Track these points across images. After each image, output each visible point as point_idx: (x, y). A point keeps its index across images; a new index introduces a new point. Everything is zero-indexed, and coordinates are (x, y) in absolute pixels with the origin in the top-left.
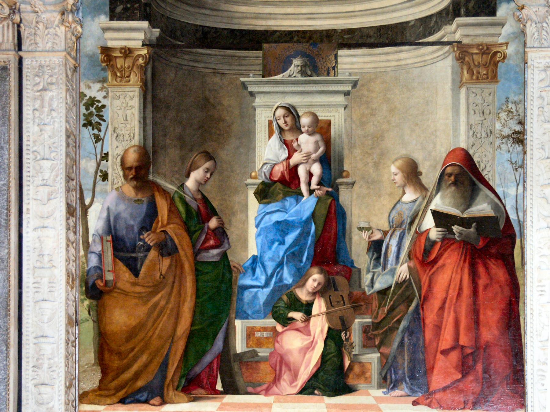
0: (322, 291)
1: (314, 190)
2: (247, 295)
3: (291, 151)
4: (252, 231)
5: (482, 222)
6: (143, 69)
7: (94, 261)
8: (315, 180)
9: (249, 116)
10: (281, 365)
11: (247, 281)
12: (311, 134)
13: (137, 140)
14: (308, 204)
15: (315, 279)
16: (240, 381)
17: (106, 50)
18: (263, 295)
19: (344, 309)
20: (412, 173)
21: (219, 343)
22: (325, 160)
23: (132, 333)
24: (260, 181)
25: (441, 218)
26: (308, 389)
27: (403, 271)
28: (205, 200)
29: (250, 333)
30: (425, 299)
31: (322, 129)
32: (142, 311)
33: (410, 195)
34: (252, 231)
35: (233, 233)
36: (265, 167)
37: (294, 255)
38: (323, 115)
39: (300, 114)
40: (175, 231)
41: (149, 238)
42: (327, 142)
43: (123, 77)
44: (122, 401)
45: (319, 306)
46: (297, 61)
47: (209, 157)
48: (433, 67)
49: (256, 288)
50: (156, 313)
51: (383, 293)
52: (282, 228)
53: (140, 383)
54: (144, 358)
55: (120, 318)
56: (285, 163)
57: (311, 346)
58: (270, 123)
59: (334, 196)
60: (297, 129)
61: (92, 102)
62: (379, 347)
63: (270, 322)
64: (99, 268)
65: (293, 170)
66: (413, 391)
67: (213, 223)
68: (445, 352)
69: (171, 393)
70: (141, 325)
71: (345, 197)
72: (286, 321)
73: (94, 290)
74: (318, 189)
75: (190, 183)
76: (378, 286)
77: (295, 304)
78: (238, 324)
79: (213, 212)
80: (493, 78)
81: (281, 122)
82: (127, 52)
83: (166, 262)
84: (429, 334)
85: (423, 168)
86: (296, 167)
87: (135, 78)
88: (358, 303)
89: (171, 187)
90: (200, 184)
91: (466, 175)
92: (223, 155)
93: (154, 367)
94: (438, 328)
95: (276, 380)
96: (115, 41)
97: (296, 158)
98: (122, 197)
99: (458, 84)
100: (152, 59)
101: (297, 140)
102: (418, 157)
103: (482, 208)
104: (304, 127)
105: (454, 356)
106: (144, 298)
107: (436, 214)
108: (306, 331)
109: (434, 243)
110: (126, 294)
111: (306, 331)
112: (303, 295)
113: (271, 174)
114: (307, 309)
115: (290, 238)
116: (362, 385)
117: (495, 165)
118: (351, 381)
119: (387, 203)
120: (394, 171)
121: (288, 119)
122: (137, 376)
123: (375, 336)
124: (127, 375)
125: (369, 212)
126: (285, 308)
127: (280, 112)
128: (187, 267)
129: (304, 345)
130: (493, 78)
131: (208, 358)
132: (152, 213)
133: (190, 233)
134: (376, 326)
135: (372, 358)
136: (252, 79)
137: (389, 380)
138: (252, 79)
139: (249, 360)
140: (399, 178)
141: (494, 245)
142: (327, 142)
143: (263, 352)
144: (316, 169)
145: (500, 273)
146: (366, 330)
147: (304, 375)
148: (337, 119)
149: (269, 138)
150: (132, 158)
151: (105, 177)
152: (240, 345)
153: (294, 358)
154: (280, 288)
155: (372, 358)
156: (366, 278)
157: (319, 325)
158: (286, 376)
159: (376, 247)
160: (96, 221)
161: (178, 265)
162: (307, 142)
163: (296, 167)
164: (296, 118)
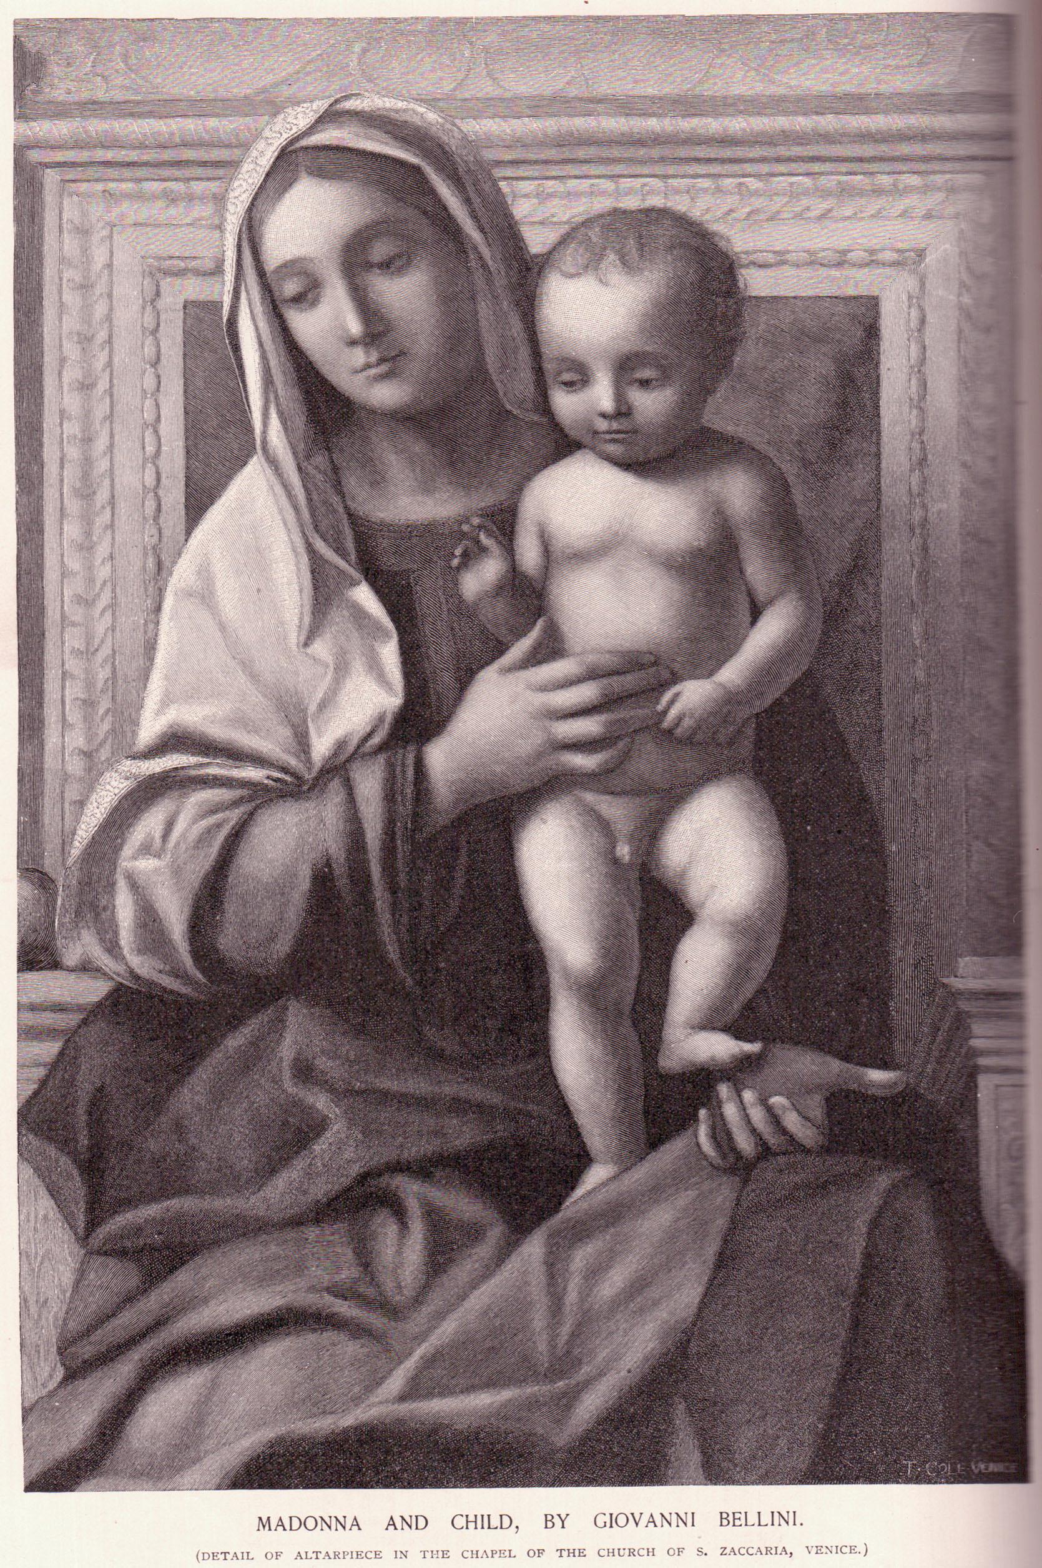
1: (702, 1081)
8: (700, 965)
12: (651, 458)
24: (94, 990)
36: (151, 823)
39: (537, 241)
56: (369, 783)
58: (209, 339)
74: (739, 1071)
81: (326, 323)
86: (496, 816)
97: (497, 716)
101: (504, 522)
104: (579, 376)
113: (210, 897)
121: (407, 294)
127: (310, 221)
144: (722, 850)
149: (198, 501)
163: (496, 816)
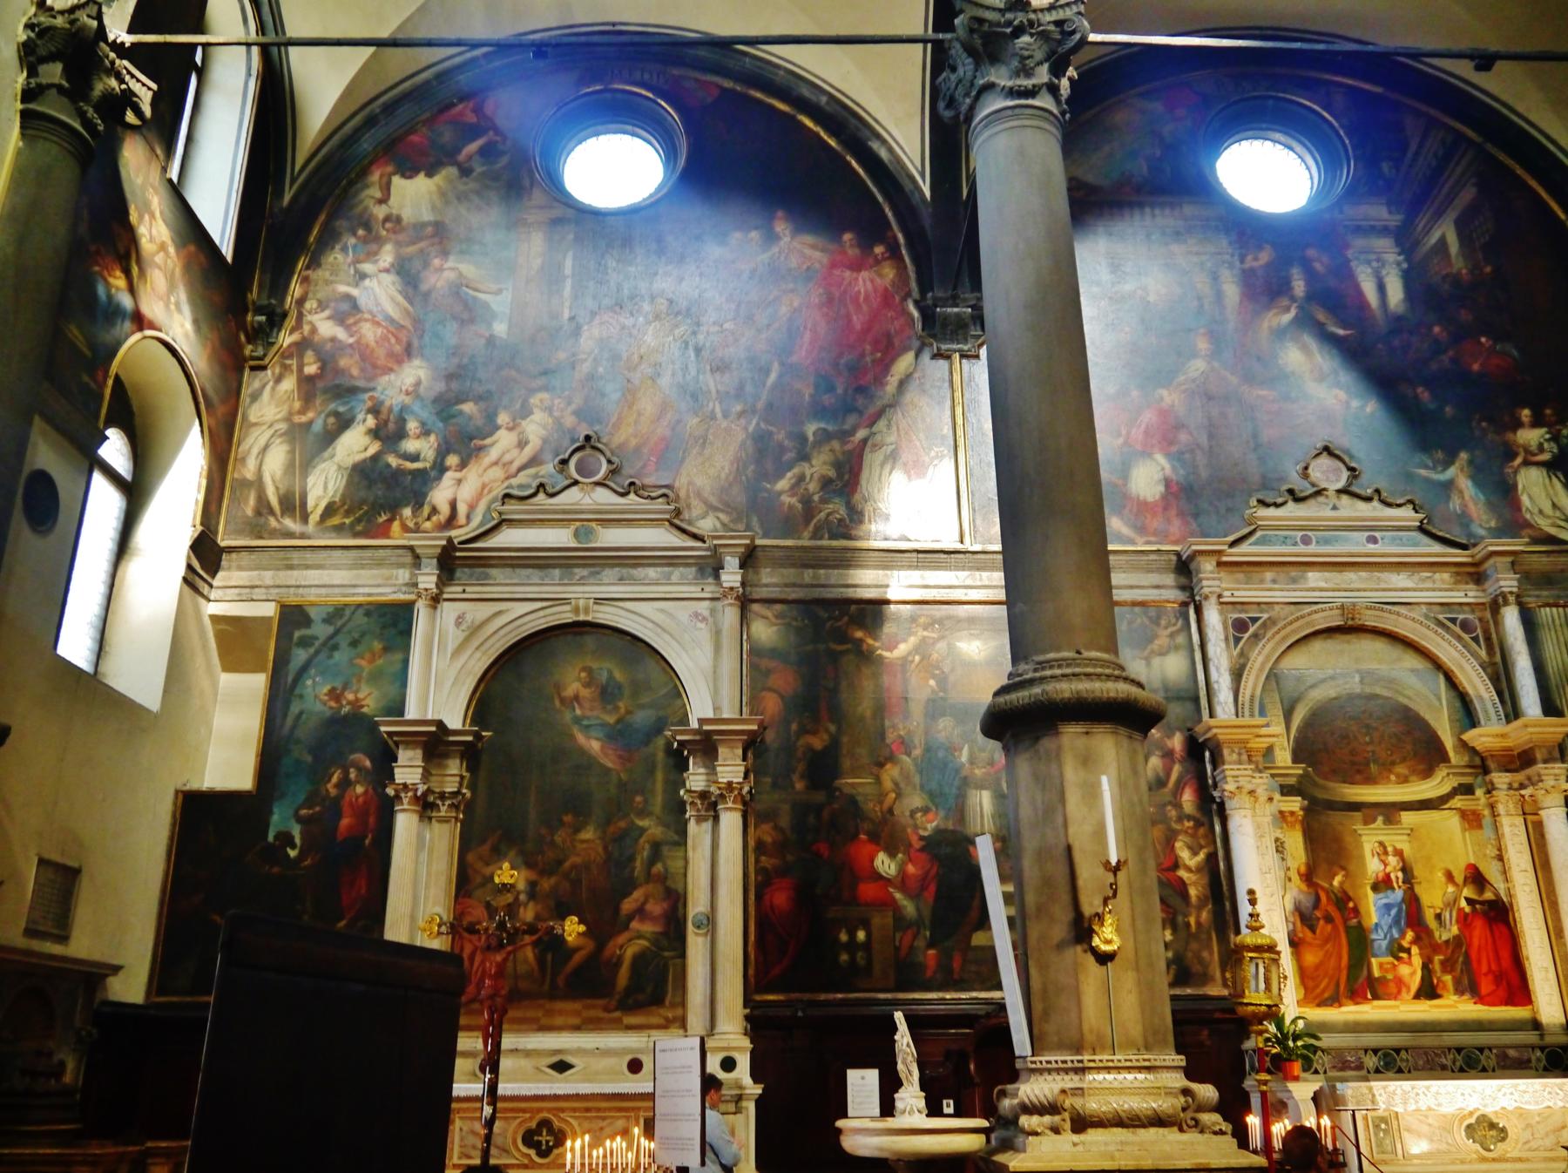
0: (1414, 942)
2: (1376, 944)
4: (1373, 909)
5: (1490, 902)
6: (1302, 822)
9: (1360, 846)
10: (1400, 982)
13: (1304, 859)
14: (1398, 895)
15: (1410, 935)
16: (1380, 992)
17: (1281, 812)
18: (1384, 944)
19: (1427, 951)
20: (1450, 877)
22: (1404, 870)
23: (1317, 967)
25: (1468, 900)
26: (1417, 996)
27: (1455, 930)
28: (1345, 892)
29: (1381, 965)
30: (1469, 946)
31: (1399, 853)
32: (1321, 954)
33: (1451, 889)
34: (1373, 909)
35: (1362, 910)
37: (1396, 921)
38: (1399, 846)
41: (1318, 914)
42: (1403, 859)
43: (1292, 826)
44: (1319, 1005)
45: (1415, 950)
46: (1380, 819)
47: (1343, 868)
48: (1447, 822)
49: (1380, 940)
50: (1328, 955)
51: (1447, 942)
52: (1388, 907)
53: (1326, 995)
55: (1311, 958)
57: (1413, 973)
59: (1412, 889)
60: (1386, 853)
62: (1450, 972)
63: (1391, 959)
65: (1388, 876)
67: (1351, 905)
69: (1344, 1001)
71: (1417, 889)
72: (1399, 959)
75: (1336, 883)
76: (1444, 938)
78: (1373, 960)
79: (1350, 899)
80: (1480, 826)
82: (1292, 813)
83: (1329, 927)
84: (1475, 964)
85: (1455, 874)
87: (1298, 827)
88: (1436, 948)
89: (1326, 885)
90: (1341, 883)
91: (1476, 878)
92: (1352, 867)
93: (1332, 986)
94: (1479, 961)
95: (1399, 992)
97: (1389, 869)
98: (1300, 891)
99: (1464, 830)
100: (1305, 816)
102: (1452, 868)
103: (1488, 895)
105: (1490, 977)
106: (1321, 946)
107: (1467, 899)
108: (1410, 963)
109: (1466, 915)
111: (1410, 963)
112: (1405, 944)
114: (1408, 951)
115: (1393, 912)
117: (1491, 871)
118: (1439, 992)
119: (1440, 893)
120: (1440, 875)
122: (1323, 991)
123: (1447, 966)
125: (1434, 895)
126: (1397, 950)
128: (1341, 929)
129: (1411, 971)
130: (1480, 826)
131: (1361, 980)
132: (1318, 899)
133: (1339, 909)
135: (1448, 978)
136: (1359, 827)
137: (1459, 991)
138: (1359, 827)
140: (1444, 879)
141: (1498, 914)
142: (1403, 859)
143: (1390, 976)
144: (1400, 875)
145: (1506, 931)
146: (1443, 963)
148: (1406, 848)
150: (1303, 869)
152: (1376, 973)
153: (1407, 979)
154: (1393, 941)
155: (1448, 978)
156: (1437, 934)
157: (1417, 961)
158: (1404, 990)
159: (1438, 917)
161: (1335, 928)
162: (1393, 860)
164: (1385, 848)
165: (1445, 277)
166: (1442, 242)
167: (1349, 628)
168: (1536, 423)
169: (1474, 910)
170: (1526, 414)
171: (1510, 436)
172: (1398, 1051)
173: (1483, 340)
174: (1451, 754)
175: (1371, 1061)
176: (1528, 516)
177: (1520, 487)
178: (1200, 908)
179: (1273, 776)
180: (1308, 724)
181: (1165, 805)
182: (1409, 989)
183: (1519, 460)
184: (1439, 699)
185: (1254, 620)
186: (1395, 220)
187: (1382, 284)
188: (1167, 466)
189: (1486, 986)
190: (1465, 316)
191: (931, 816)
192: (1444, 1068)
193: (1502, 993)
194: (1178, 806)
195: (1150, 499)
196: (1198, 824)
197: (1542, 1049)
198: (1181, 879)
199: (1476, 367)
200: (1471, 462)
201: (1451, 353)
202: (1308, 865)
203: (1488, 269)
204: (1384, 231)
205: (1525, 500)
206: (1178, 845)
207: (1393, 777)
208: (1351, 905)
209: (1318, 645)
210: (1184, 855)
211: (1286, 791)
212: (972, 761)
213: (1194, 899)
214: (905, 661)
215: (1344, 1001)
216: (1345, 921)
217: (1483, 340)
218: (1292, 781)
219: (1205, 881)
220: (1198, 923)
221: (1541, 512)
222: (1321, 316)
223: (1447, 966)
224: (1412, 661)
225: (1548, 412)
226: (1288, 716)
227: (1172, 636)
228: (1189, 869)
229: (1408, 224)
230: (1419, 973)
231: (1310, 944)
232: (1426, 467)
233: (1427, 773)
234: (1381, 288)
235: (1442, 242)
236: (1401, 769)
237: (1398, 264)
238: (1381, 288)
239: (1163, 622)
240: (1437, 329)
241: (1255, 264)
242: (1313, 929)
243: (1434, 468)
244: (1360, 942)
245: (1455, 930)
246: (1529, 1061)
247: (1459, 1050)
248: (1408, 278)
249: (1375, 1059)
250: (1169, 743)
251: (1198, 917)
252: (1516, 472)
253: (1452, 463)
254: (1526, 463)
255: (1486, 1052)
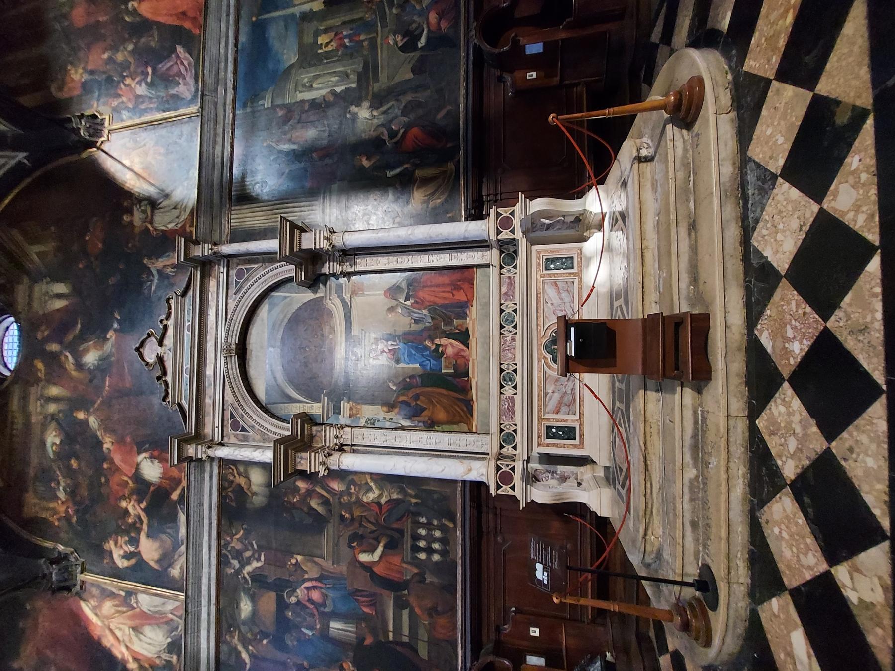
3: (384, 351)
4: (411, 366)
7: (421, 424)
10: (458, 355)
11: (428, 367)
15: (428, 343)
17: (350, 417)
20: (391, 309)
21: (450, 378)
23: (447, 411)
27: (425, 312)
29: (447, 367)
30: (435, 303)
40: (411, 393)
43: (358, 411)
45: (437, 341)
49: (430, 364)
54: (457, 407)
55: (441, 415)
57: (451, 344)
61: (366, 422)
64: (423, 422)
66: (468, 307)
68: (454, 295)
69: (469, 397)
70: (444, 408)
72: (443, 353)
73: (430, 426)
75: (394, 388)
77: (436, 350)
82: (351, 409)
83: (421, 397)
87: (359, 407)
88: (436, 327)
93: (459, 403)
94: (445, 298)
95: (464, 357)
96: (347, 414)
98: (398, 413)
106: (434, 406)
109: (416, 302)
110: (432, 413)
112: (433, 347)
114: (438, 346)
115: (413, 352)
116: (465, 326)
118: (464, 329)
122: (463, 410)
124: (462, 413)
126: (438, 354)
129: (451, 347)
134: (444, 320)
137: (464, 316)
139: (456, 367)
144: (390, 343)
146: (446, 324)
147: (462, 347)
150: (385, 409)
151: (392, 419)
153: (456, 351)
156: (427, 324)
157: (444, 341)
158: (463, 354)
160: (406, 423)
161: (421, 394)
165: (55, 256)
166: (38, 254)
167: (241, 351)
168: (130, 212)
169: (414, 296)
170: (126, 218)
171: (137, 230)
172: (502, 371)
173: (87, 238)
174: (318, 295)
175: (508, 391)
176: (179, 226)
177: (164, 228)
178: (406, 494)
179: (328, 418)
180: (297, 388)
181: (340, 502)
182: (463, 350)
183: (149, 226)
184: (286, 297)
185: (232, 416)
186: (26, 280)
187: (55, 297)
188: (144, 455)
189: (461, 296)
190: (75, 247)
191: (344, 665)
192: (513, 340)
193: (466, 286)
194: (341, 494)
195: (161, 470)
196: (353, 482)
197: (501, 268)
198: (386, 502)
199: (100, 245)
200: (150, 258)
201: (93, 260)
202: (383, 404)
203: (53, 228)
204: (31, 289)
205: (170, 226)
206: (365, 500)
207: (331, 337)
208: (408, 380)
209: (252, 372)
210: (371, 496)
211: (337, 411)
212: (311, 628)
213: (400, 496)
214: (252, 656)
215: (469, 397)
216: (417, 386)
217: (87, 238)
218: (331, 405)
219: (388, 485)
220: (415, 497)
221: (177, 217)
222: (70, 337)
223: (448, 321)
224: (263, 311)
225: (125, 204)
226: (292, 400)
227: (239, 474)
228: (381, 496)
229: (28, 273)
230: (451, 341)
231: (432, 413)
232: (151, 286)
233: (330, 314)
234: (59, 296)
235: (38, 254)
236: (326, 329)
237: (47, 283)
238: (59, 296)
239: (232, 478)
240: (80, 266)
241: (43, 372)
242: (423, 409)
243: (151, 281)
244: (431, 379)
245: (425, 312)
246: (509, 278)
247: (502, 327)
248: (56, 279)
249: (507, 388)
250: (303, 491)
251: (411, 495)
252: (155, 230)
253: (149, 268)
254: (151, 223)
255: (503, 307)
